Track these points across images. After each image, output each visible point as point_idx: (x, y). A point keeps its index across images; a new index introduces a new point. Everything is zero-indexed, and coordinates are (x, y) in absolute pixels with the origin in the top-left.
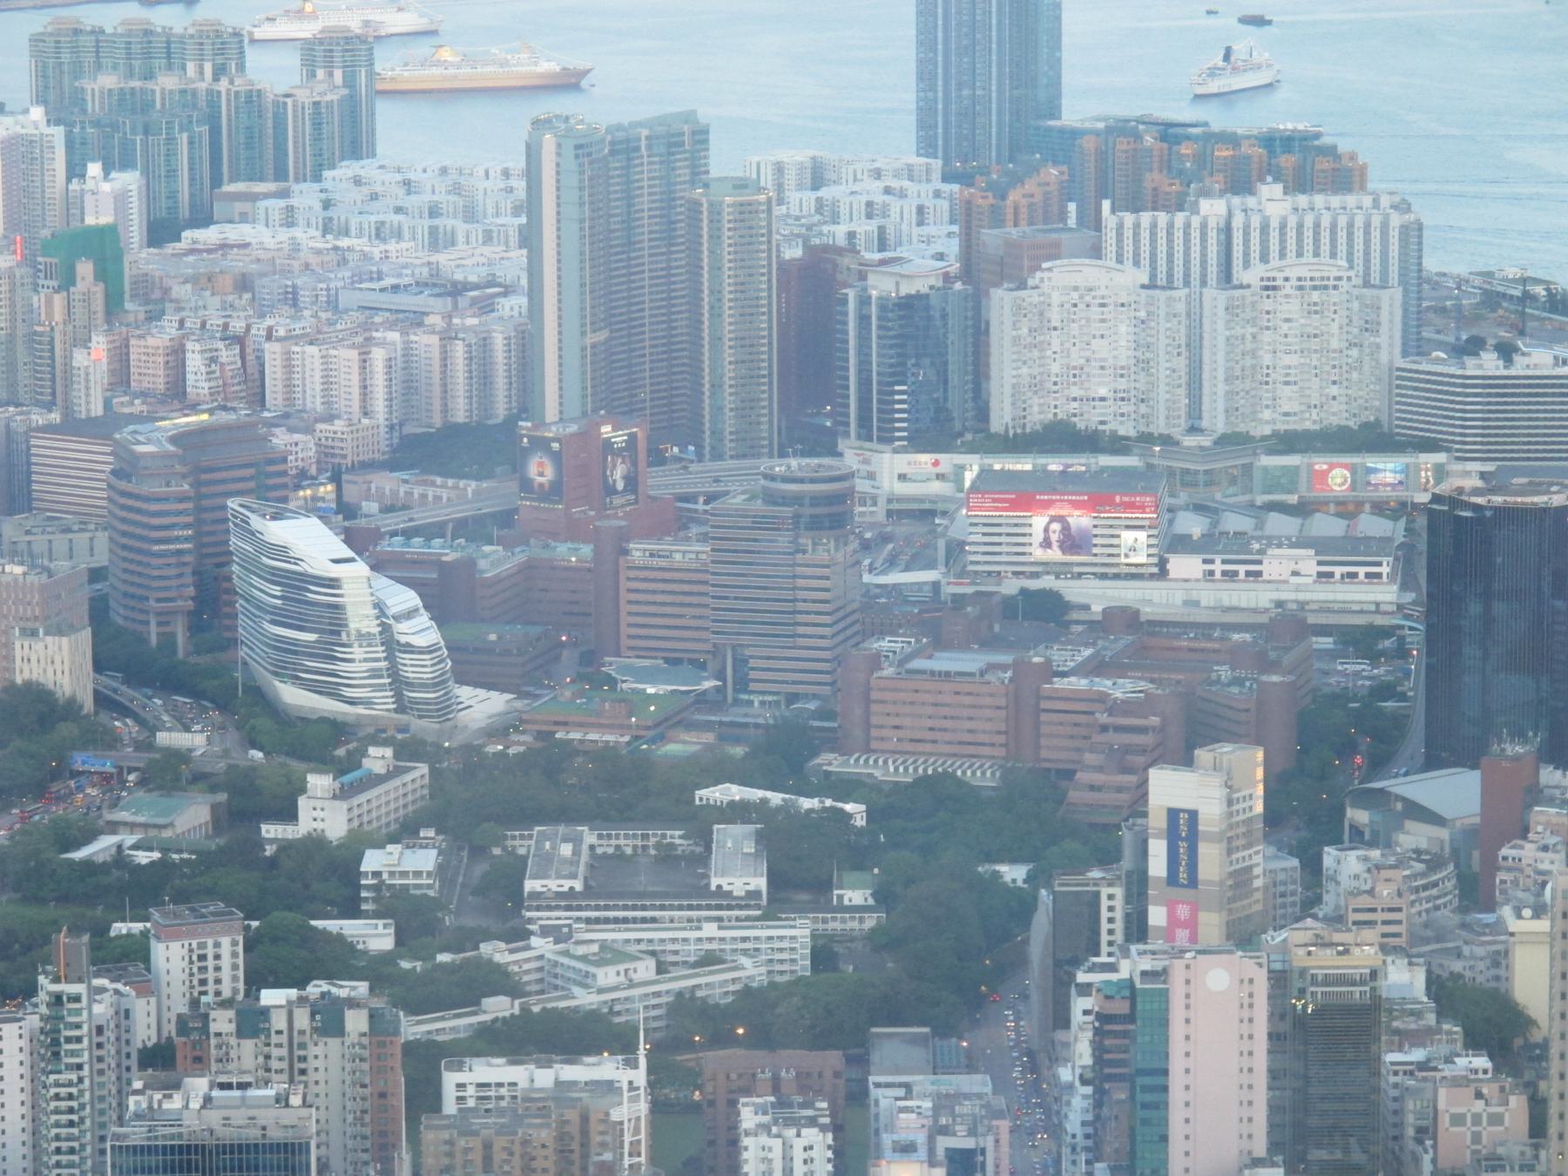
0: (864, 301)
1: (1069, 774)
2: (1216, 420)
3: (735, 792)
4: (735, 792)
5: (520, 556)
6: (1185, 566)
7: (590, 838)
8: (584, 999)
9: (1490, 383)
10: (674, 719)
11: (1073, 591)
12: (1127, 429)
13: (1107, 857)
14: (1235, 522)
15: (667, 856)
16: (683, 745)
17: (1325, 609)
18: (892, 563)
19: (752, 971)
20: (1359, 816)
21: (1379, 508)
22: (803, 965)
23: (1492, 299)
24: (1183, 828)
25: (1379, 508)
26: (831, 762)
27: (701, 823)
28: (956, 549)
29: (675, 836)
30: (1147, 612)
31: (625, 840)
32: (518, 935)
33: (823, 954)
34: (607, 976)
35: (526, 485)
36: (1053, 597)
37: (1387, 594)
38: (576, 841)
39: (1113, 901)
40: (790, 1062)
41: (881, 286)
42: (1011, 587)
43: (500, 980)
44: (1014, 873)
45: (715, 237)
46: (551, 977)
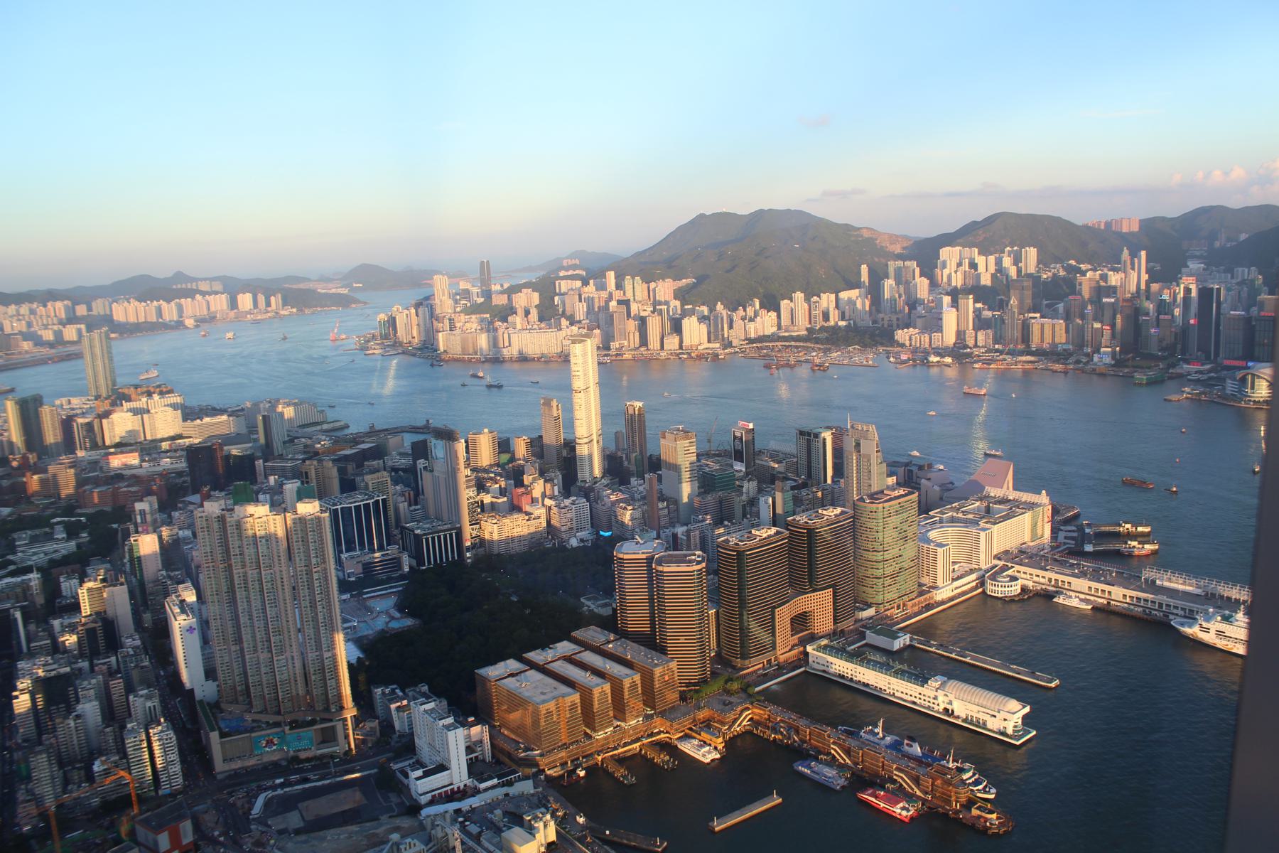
0: (77, 424)
1: (125, 506)
2: (149, 437)
3: (59, 519)
4: (59, 519)
5: (11, 481)
6: (143, 464)
7: (29, 532)
8: (29, 563)
9: (199, 426)
10: (47, 507)
11: (124, 472)
12: (132, 442)
13: (130, 520)
14: (154, 456)
15: (46, 534)
16: (49, 512)
17: (173, 469)
18: (89, 472)
19: (64, 552)
20: (180, 505)
21: (182, 450)
22: (75, 549)
23: (201, 410)
24: (143, 513)
25: (182, 450)
26: (79, 511)
27: (52, 526)
28: (101, 468)
29: (47, 530)
30: (138, 474)
31: (37, 532)
32: (14, 553)
33: (79, 546)
34: (34, 558)
35: (12, 467)
36: (121, 474)
37: (184, 465)
38: (26, 533)
39: (132, 528)
40: (69, 568)
41: (81, 421)
42: (112, 473)
43: (12, 563)
44: (115, 526)
45: (46, 416)
46: (23, 560)
